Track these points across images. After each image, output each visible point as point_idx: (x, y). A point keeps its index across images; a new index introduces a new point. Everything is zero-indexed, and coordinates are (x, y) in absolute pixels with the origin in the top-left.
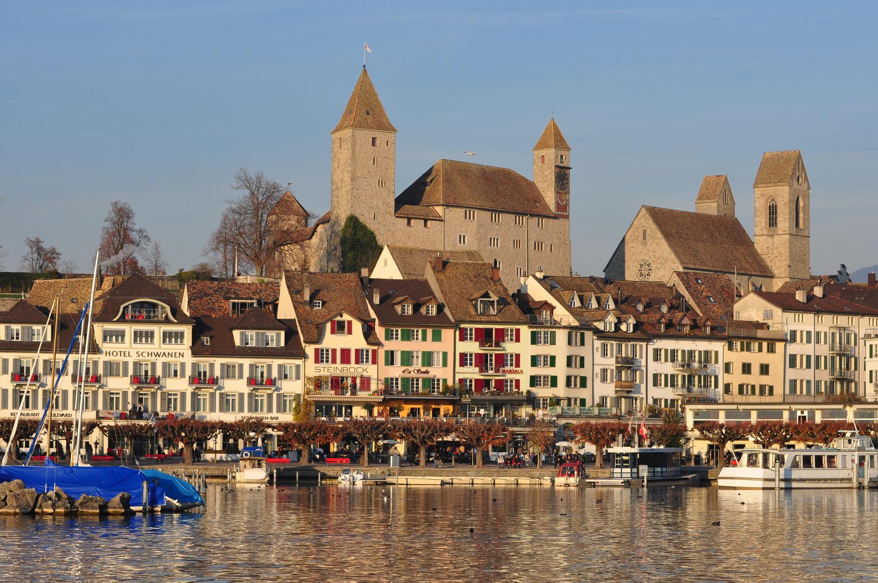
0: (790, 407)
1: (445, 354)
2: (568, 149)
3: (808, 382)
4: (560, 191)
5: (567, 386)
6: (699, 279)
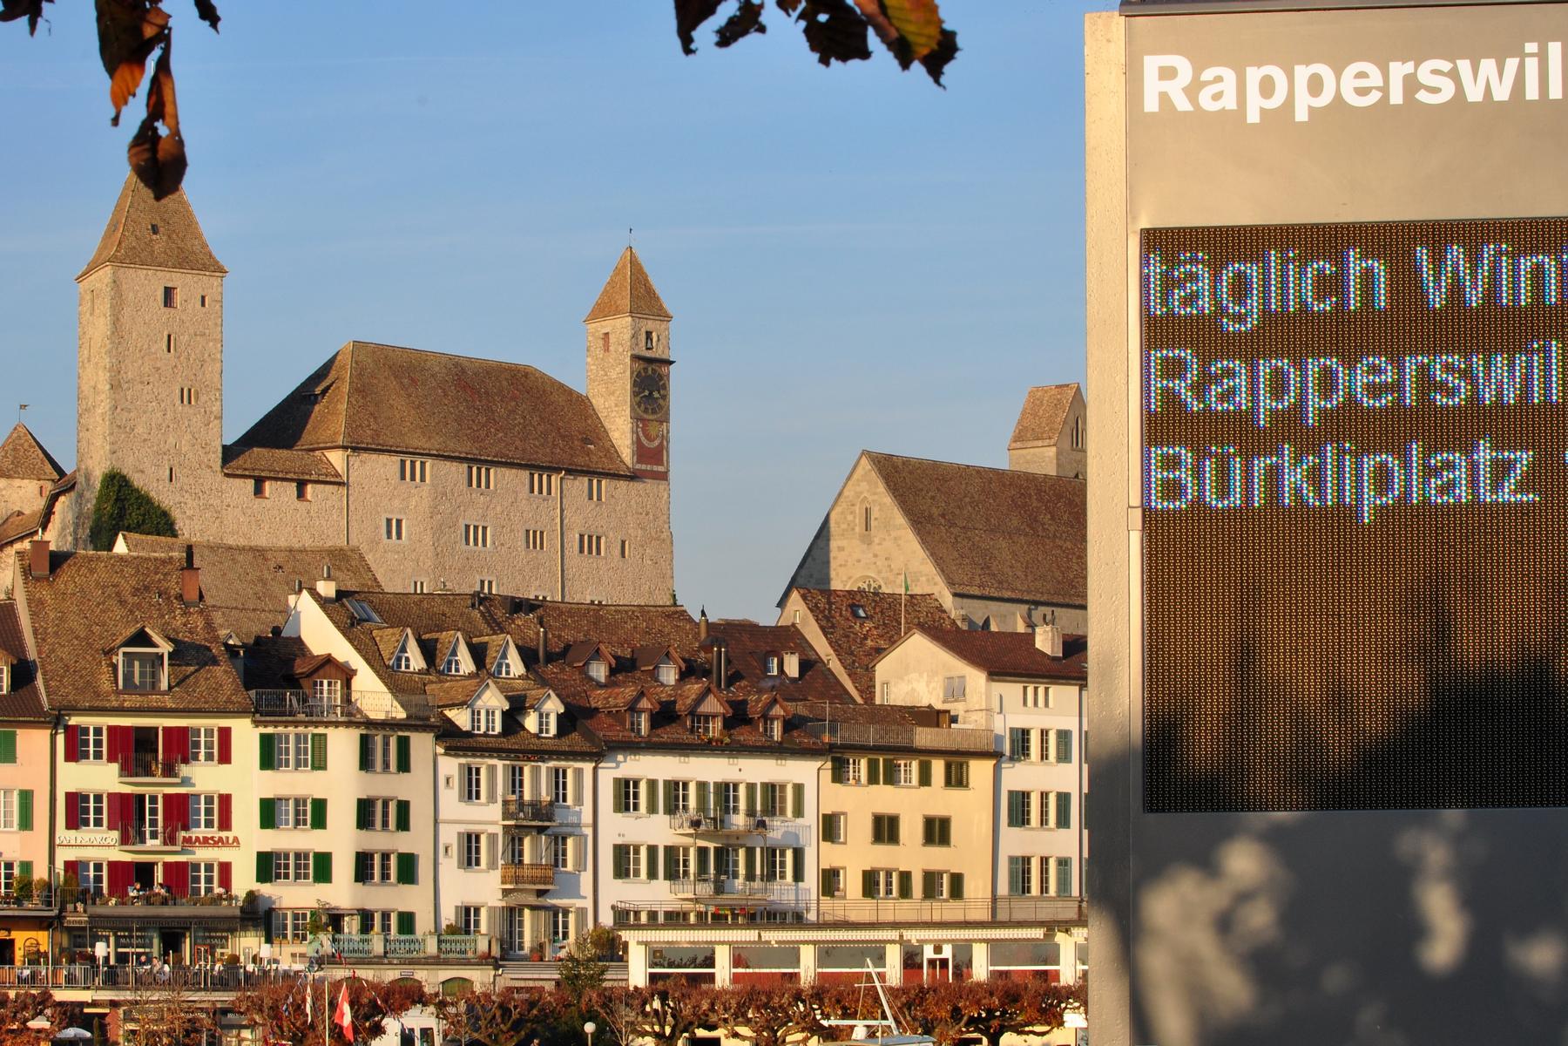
0: (901, 936)
1: (26, 797)
2: (664, 316)
3: (1063, 863)
4: (645, 416)
5: (357, 880)
6: (859, 606)
